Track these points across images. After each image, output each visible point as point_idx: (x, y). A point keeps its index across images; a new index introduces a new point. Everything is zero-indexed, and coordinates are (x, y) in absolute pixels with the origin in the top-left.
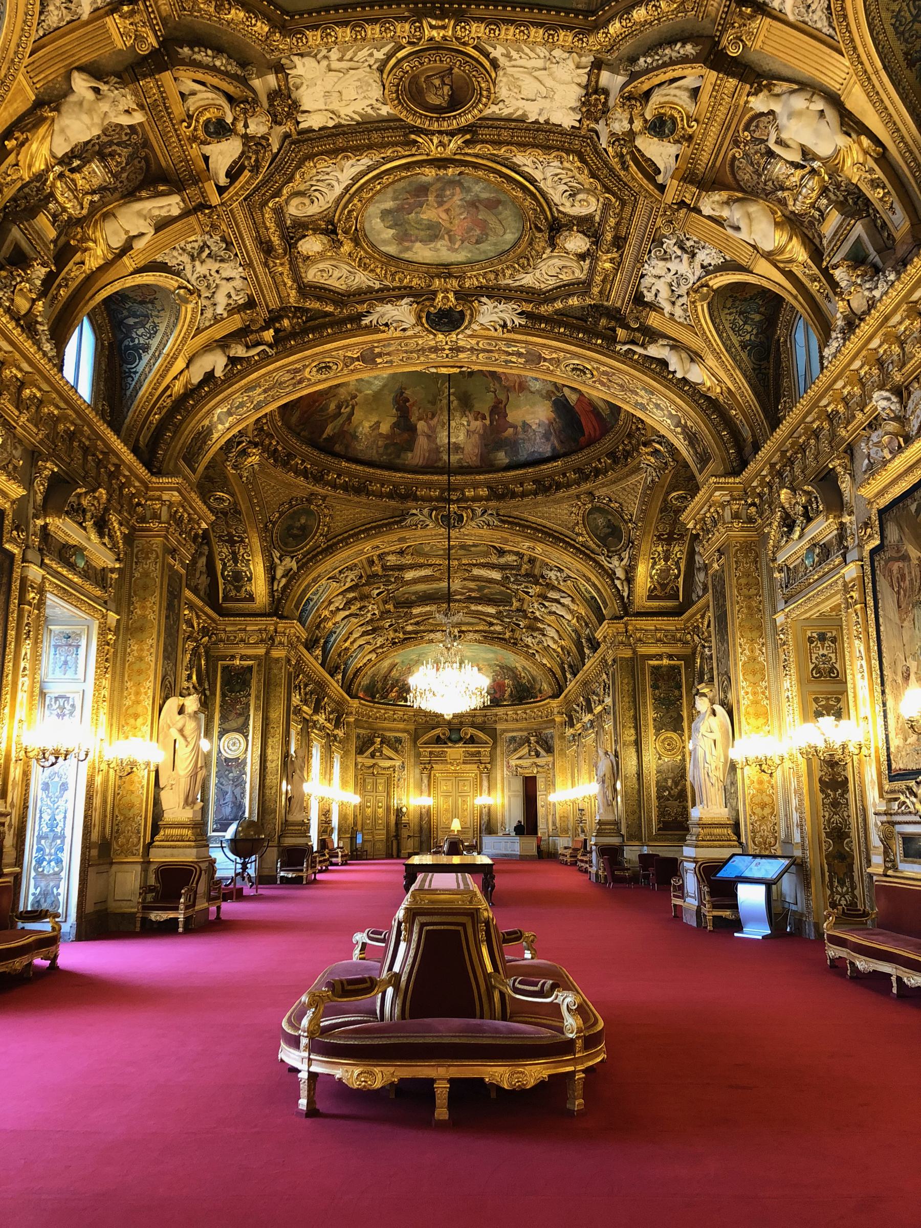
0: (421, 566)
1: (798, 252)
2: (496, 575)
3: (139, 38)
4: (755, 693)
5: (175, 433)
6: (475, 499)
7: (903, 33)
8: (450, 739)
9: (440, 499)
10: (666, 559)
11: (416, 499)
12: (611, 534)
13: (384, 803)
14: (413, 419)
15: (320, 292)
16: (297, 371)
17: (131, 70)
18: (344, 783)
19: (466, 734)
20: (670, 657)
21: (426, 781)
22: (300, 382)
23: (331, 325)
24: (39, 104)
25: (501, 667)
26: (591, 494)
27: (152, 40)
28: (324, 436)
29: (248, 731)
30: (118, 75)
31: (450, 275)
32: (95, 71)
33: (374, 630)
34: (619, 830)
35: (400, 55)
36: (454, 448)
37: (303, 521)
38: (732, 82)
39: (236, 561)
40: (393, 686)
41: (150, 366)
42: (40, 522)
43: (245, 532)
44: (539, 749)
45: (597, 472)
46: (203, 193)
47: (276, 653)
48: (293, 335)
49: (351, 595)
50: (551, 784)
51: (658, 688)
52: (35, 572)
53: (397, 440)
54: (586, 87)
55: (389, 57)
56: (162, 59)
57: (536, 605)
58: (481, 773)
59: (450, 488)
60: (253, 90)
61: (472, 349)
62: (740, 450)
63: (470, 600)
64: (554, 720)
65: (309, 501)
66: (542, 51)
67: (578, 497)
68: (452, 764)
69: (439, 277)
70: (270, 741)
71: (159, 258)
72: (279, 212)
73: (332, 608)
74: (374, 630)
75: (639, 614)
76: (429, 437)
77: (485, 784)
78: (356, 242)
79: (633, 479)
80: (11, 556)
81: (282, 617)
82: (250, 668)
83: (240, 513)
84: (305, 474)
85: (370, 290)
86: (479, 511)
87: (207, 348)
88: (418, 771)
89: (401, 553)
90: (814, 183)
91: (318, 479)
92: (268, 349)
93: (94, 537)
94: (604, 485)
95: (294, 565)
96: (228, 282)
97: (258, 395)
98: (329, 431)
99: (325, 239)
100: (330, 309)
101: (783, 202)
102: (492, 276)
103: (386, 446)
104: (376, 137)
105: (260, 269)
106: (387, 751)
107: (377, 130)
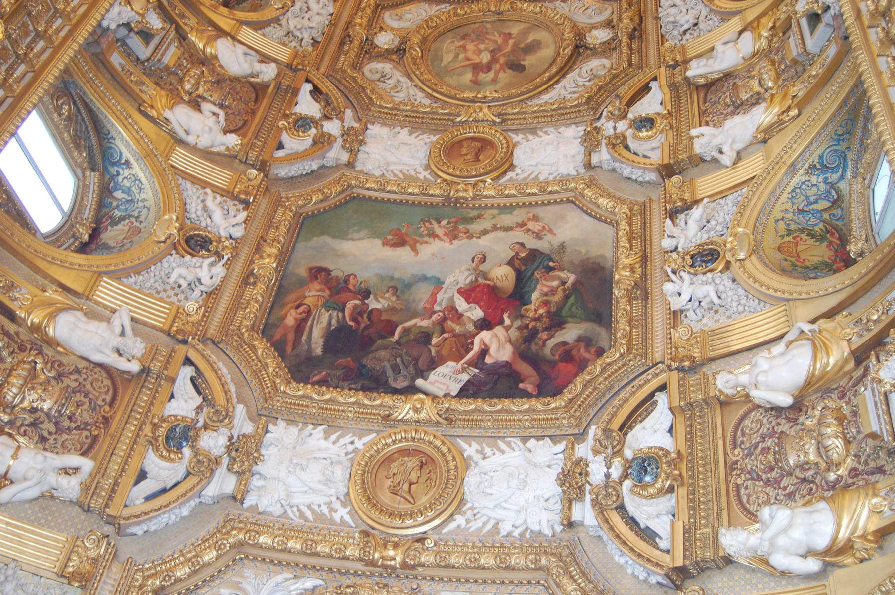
7: (136, 180)
35: (495, 174)
66: (389, 176)
90: (188, 87)
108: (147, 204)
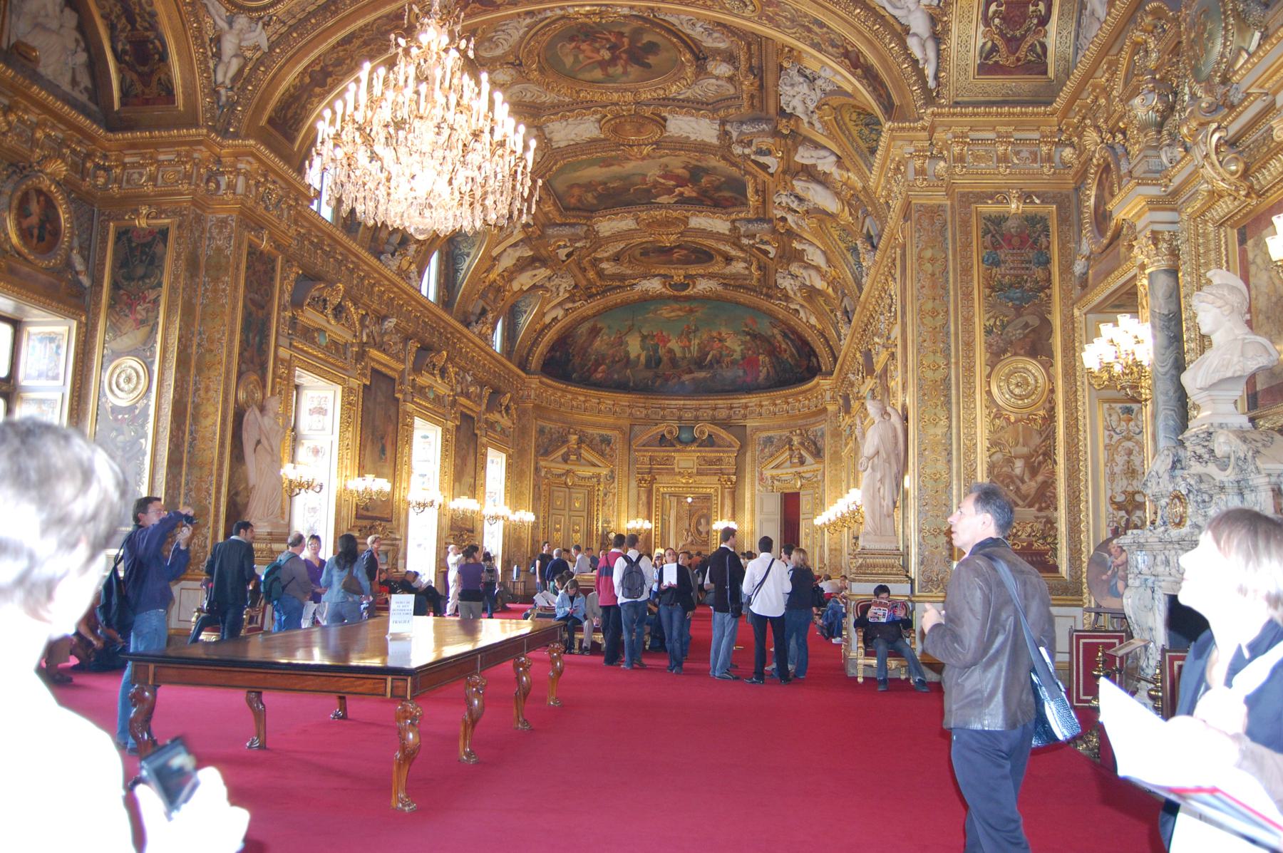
8: (681, 442)
13: (583, 527)
19: (702, 432)
20: (1026, 197)
21: (644, 498)
29: (153, 355)
34: (906, 568)
40: (598, 363)
50: (820, 505)
51: (997, 263)
58: (723, 488)
64: (825, 410)
77: (728, 502)
82: (164, 233)
106: (586, 454)
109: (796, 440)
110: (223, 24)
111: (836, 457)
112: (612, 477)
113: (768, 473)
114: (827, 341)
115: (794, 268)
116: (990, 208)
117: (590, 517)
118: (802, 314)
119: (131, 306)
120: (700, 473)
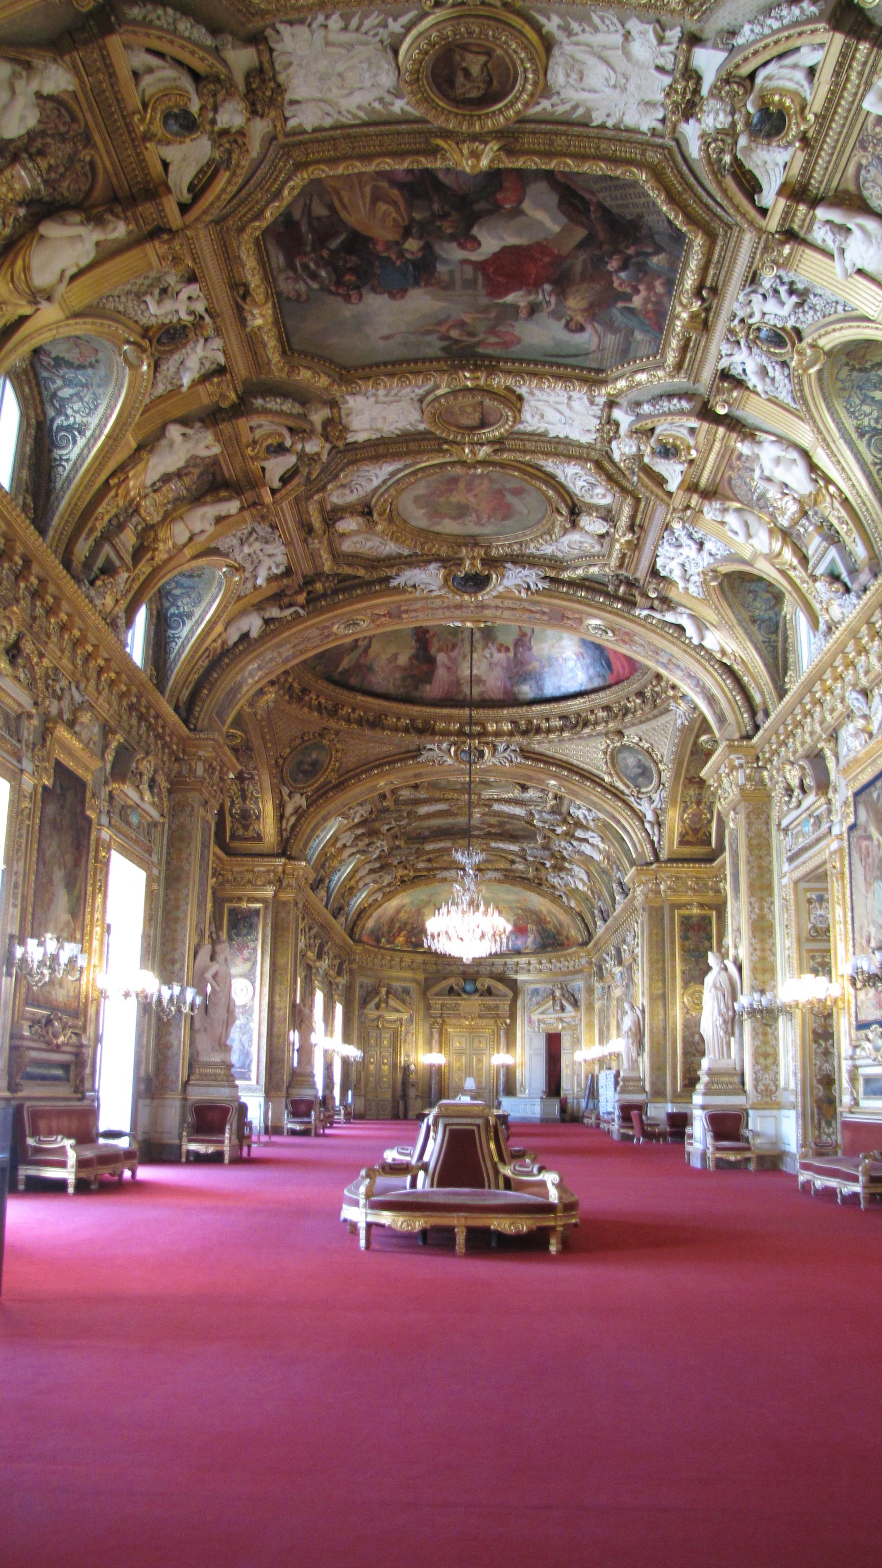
0: (437, 800)
1: (788, 555)
2: (519, 811)
3: (223, 396)
4: (763, 950)
5: (210, 691)
6: (498, 734)
9: (460, 733)
10: (698, 803)
11: (433, 733)
12: (642, 774)
14: (433, 651)
15: (354, 559)
16: (325, 628)
17: (213, 417)
18: (347, 1038)
20: (701, 906)
21: (436, 1036)
22: (328, 637)
23: (361, 586)
24: (140, 448)
25: (525, 910)
26: (620, 733)
27: (233, 396)
28: (340, 669)
30: (202, 420)
31: (476, 544)
32: (184, 421)
33: (382, 868)
35: (439, 392)
36: (473, 680)
37: (314, 756)
38: (721, 430)
39: (244, 798)
40: (401, 930)
41: (192, 631)
42: (108, 789)
43: (255, 768)
44: (564, 1002)
45: (626, 711)
46: (259, 496)
47: (287, 896)
48: (324, 596)
49: (360, 831)
50: (576, 1042)
52: (106, 834)
53: (416, 672)
54: (600, 418)
55: (428, 393)
56: (241, 408)
57: (563, 843)
58: (498, 1029)
59: (471, 722)
60: (311, 423)
61: (497, 607)
62: (753, 713)
63: (490, 836)
65: (321, 735)
67: (606, 735)
68: (466, 1018)
69: (466, 545)
70: (277, 988)
71: (213, 545)
72: (321, 503)
73: (339, 845)
74: (382, 868)
75: (671, 860)
76: (449, 669)
77: (503, 1040)
78: (391, 520)
79: (662, 720)
80: (89, 821)
81: (290, 858)
82: (257, 912)
83: (251, 750)
84: (319, 708)
85: (399, 556)
86: (501, 748)
87: (243, 613)
88: (427, 1026)
89: (416, 787)
91: (333, 712)
92: (301, 611)
93: (147, 796)
94: (633, 725)
95: (304, 803)
96: (271, 559)
97: (287, 651)
98: (345, 663)
99: (360, 520)
100: (361, 572)
101: (772, 515)
102: (516, 547)
103: (404, 679)
104: (413, 446)
105: (299, 545)
106: (393, 1002)
107: (414, 440)
108: (839, 385)
109: (558, 993)
110: (286, 798)
111: (590, 1007)
112: (411, 1020)
113: (535, 1017)
114: (583, 919)
115: (563, 875)
116: (685, 912)
117: (395, 1052)
118: (565, 899)
119: (240, 950)
120: (481, 1017)
